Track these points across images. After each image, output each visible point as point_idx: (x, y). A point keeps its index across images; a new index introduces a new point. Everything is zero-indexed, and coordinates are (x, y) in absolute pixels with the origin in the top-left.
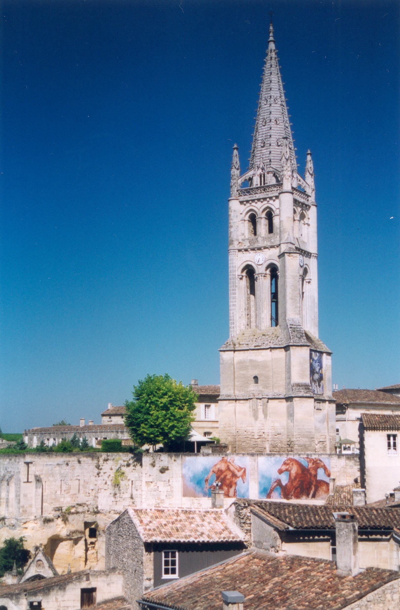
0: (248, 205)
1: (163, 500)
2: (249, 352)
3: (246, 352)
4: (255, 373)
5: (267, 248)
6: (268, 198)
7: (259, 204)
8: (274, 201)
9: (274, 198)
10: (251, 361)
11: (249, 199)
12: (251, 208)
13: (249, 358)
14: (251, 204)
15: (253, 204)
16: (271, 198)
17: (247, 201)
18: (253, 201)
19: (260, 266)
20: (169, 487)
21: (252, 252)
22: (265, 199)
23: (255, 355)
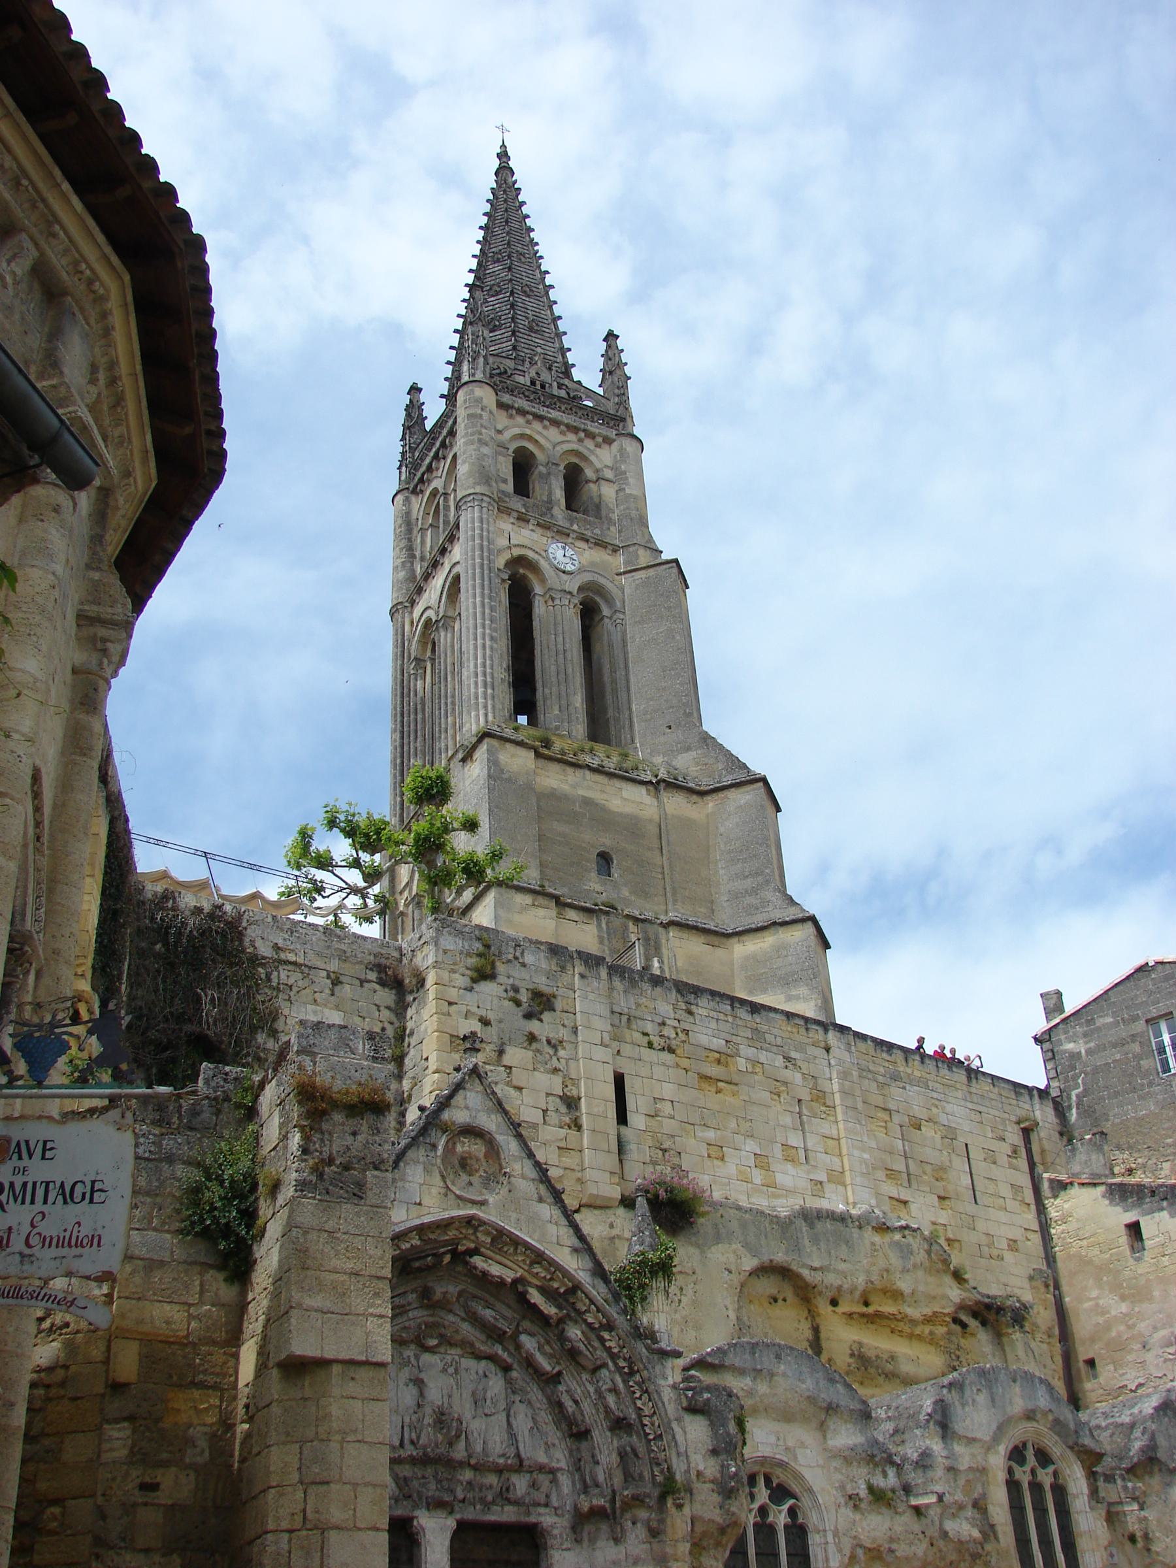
0: (520, 420)
1: (535, 1126)
2: (579, 773)
3: (570, 770)
4: (606, 841)
5: (587, 541)
6: (584, 430)
7: (553, 434)
8: (598, 446)
9: (600, 440)
10: (587, 802)
11: (527, 408)
12: (528, 432)
13: (581, 792)
14: (528, 422)
15: (537, 425)
16: (591, 436)
17: (522, 412)
18: (539, 418)
19: (565, 577)
20: (557, 1080)
21: (539, 530)
22: (575, 430)
23: (603, 791)
